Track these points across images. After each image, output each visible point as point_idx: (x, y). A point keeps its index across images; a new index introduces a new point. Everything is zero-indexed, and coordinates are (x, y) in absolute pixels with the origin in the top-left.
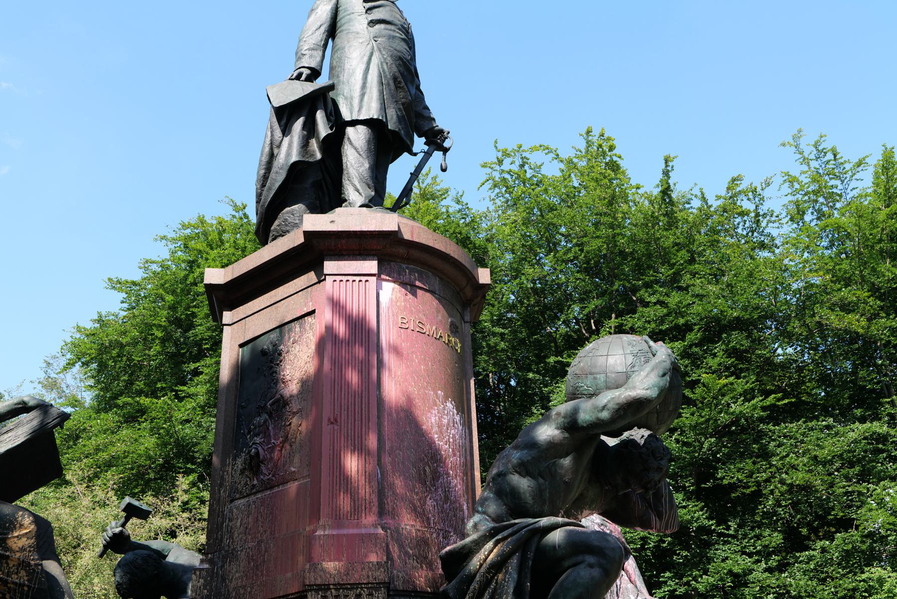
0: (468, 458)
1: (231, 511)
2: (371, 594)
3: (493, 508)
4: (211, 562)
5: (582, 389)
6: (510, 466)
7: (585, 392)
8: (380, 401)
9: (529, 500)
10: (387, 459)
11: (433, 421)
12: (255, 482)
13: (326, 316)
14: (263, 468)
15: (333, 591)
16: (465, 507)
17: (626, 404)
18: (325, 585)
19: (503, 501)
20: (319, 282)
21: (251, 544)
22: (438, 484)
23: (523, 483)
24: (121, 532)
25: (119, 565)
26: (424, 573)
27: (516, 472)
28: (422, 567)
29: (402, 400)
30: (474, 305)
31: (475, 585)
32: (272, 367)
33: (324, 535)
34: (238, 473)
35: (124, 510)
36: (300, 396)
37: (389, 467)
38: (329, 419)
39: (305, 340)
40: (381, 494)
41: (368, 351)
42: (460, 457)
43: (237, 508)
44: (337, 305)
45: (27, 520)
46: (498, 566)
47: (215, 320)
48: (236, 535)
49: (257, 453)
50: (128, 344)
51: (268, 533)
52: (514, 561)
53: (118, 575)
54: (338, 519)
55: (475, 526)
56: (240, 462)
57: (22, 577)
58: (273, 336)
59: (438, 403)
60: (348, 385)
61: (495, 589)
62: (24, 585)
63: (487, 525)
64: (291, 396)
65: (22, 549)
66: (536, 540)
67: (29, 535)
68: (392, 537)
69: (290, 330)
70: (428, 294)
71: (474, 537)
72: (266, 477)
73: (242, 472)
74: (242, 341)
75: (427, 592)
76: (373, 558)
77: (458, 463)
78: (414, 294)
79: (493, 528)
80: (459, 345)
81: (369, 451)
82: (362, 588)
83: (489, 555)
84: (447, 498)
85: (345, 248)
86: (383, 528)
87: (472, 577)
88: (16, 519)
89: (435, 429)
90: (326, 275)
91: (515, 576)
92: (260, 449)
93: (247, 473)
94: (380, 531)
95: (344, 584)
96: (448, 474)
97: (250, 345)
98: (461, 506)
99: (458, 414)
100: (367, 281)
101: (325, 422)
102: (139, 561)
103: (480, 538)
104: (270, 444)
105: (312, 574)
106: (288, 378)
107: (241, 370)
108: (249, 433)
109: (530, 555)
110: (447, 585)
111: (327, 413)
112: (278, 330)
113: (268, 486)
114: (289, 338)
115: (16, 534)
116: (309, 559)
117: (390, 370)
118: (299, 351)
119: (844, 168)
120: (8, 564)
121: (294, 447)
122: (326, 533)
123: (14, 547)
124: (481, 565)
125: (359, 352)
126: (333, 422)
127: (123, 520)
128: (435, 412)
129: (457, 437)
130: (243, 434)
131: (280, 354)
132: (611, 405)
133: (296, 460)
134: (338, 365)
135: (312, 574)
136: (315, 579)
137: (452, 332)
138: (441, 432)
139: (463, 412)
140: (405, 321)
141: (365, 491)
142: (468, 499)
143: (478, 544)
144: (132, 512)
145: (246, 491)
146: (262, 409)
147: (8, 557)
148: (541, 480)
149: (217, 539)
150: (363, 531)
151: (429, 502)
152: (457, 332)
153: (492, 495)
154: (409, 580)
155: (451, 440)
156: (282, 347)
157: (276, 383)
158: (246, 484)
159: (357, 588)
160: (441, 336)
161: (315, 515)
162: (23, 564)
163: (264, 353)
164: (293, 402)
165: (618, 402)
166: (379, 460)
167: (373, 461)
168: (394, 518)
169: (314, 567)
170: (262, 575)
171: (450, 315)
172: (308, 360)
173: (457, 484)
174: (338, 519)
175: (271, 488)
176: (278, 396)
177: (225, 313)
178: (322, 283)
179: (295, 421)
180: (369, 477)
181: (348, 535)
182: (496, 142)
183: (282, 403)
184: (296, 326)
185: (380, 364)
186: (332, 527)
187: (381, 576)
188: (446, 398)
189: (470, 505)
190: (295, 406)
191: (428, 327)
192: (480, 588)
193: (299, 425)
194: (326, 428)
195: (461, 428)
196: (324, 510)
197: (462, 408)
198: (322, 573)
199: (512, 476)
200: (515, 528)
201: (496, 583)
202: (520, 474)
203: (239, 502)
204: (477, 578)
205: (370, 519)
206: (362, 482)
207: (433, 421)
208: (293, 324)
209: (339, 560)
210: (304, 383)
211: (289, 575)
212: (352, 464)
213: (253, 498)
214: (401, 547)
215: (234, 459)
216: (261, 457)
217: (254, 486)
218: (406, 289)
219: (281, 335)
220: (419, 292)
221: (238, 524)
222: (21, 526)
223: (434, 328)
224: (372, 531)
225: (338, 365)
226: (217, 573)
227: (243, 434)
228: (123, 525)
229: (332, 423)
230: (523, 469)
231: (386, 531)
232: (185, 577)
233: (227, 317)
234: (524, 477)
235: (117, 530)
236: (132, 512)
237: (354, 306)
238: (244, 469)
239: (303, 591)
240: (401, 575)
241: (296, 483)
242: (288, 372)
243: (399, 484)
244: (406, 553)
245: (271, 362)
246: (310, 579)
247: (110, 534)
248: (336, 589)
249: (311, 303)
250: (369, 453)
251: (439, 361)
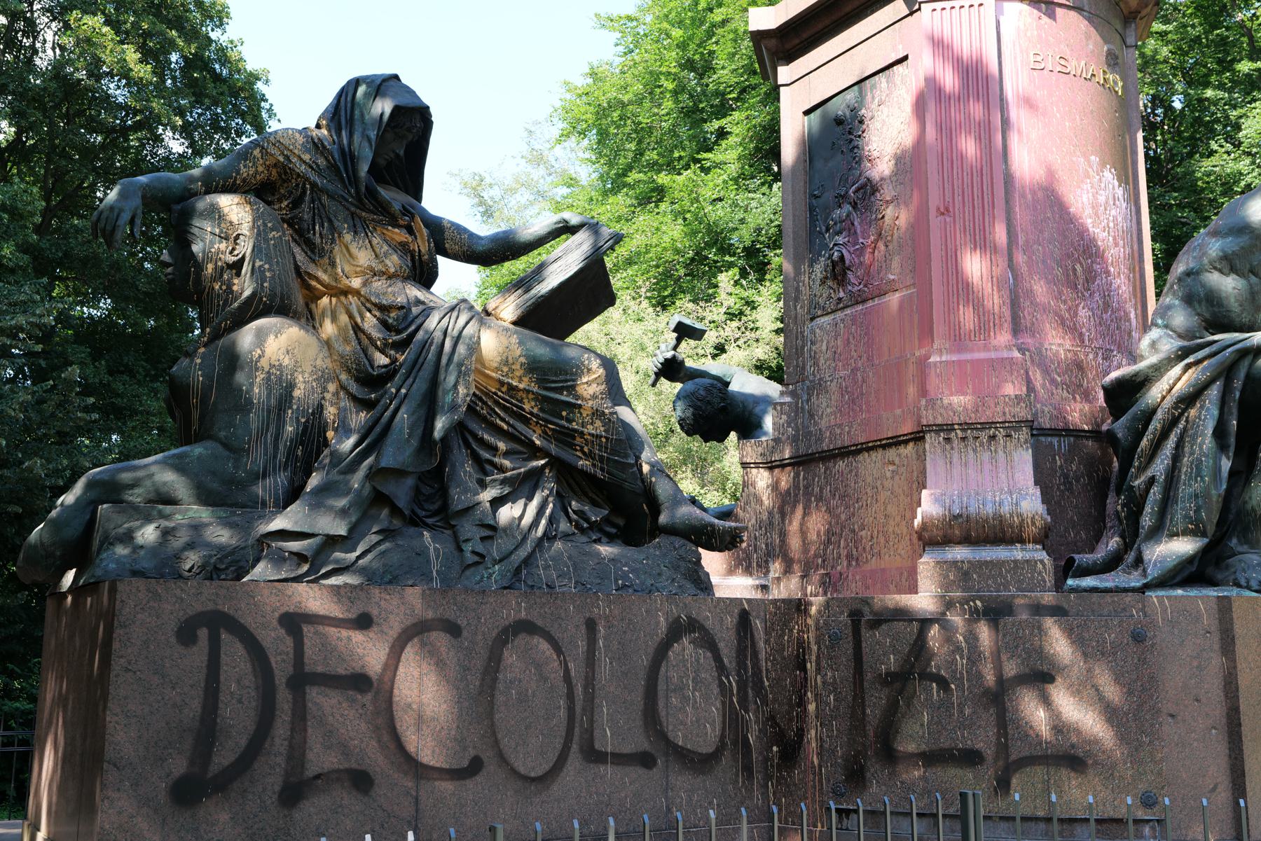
0: (1136, 247)
1: (813, 332)
2: (1009, 436)
3: (1181, 318)
4: (793, 394)
6: (1205, 261)
8: (1009, 179)
9: (1234, 306)
10: (1020, 258)
11: (1085, 200)
12: (842, 294)
13: (924, 63)
14: (850, 275)
15: (958, 432)
16: (1132, 315)
18: (947, 425)
19: (1195, 310)
20: (911, 14)
21: (842, 373)
22: (1094, 287)
23: (1228, 285)
24: (674, 356)
25: (678, 397)
26: (1078, 406)
27: (1215, 268)
28: (1074, 398)
29: (1040, 174)
30: (1141, 19)
31: (1155, 425)
32: (851, 140)
33: (941, 362)
34: (818, 282)
35: (674, 331)
36: (894, 179)
37: (1024, 269)
38: (938, 209)
40: (1015, 305)
41: (988, 107)
42: (1124, 247)
43: (821, 328)
44: (939, 45)
45: (595, 364)
46: (1190, 399)
47: (765, 77)
48: (822, 361)
49: (842, 258)
50: (630, 103)
51: (864, 358)
52: (1214, 392)
53: (678, 408)
54: (958, 340)
55: (1153, 344)
56: (819, 269)
57: (597, 428)
58: (850, 96)
59: (1091, 173)
60: (962, 157)
61: (1185, 430)
62: (601, 437)
63: (1169, 345)
64: (882, 179)
65: (594, 397)
66: (1246, 362)
67: (599, 381)
68: (1032, 361)
69: (873, 87)
70: (1073, 14)
71: (1153, 359)
72: (856, 288)
73: (823, 282)
75: (1084, 431)
76: (1010, 389)
77: (1122, 255)
78: (1052, 16)
79: (1181, 349)
80: (1120, 84)
81: (995, 245)
82: (996, 428)
83: (1175, 384)
84: (1107, 305)
86: (1019, 350)
87: (1150, 413)
88: (582, 363)
89: (1088, 211)
90: (920, 3)
91: (1216, 412)
92: (844, 251)
93: (830, 283)
94: (1016, 354)
95: (972, 424)
96: (1108, 273)
97: (818, 112)
98: (1127, 314)
99: (1120, 186)
101: (933, 212)
102: (702, 392)
103: (1160, 362)
104: (857, 243)
105: (930, 412)
106: (875, 154)
107: (811, 148)
108: (828, 230)
109: (1238, 384)
110: (1113, 423)
111: (934, 202)
112: (856, 88)
113: (860, 299)
114: (873, 98)
115: (585, 380)
116: (923, 392)
117: (1019, 131)
120: (581, 414)
121: (890, 247)
122: (944, 358)
123: (585, 394)
124: (1164, 398)
125: (976, 110)
126: (944, 211)
127: (674, 342)
128: (1087, 186)
129: (1120, 219)
130: (820, 232)
131: (861, 122)
133: (896, 263)
134: (947, 132)
135: (930, 412)
137: (1109, 65)
138: (1096, 215)
139: (1127, 183)
140: (1039, 59)
141: (995, 301)
142: (1135, 304)
143: (1159, 370)
144: (684, 332)
145: (830, 306)
146: (841, 199)
147: (580, 406)
148: (1253, 279)
149: (797, 366)
150: (993, 355)
151: (1083, 313)
152: (1117, 64)
153: (1177, 302)
154: (1060, 414)
155: (1111, 225)
156: (863, 111)
157: (859, 162)
158: (830, 297)
159: (990, 428)
160: (1093, 75)
161: (927, 332)
162: (598, 414)
163: (839, 121)
164: (885, 187)
166: (1010, 259)
167: (1002, 262)
168: (1034, 336)
169: (932, 403)
170: (861, 410)
171: (1106, 42)
172: (902, 127)
173: (1122, 284)
174: (958, 340)
175: (864, 301)
176: (862, 180)
177: (780, 69)
179: (889, 212)
180: (999, 284)
181: (972, 362)
183: (870, 189)
184: (881, 79)
185: (1006, 123)
186: (950, 351)
187: (1022, 412)
188: (1103, 165)
189: (1139, 312)
190: (887, 192)
191: (1074, 63)
192: (1163, 427)
193: (897, 217)
194: (935, 221)
195: (1124, 205)
196: (939, 328)
197: (1126, 177)
198: (942, 411)
199: (1208, 274)
200: (1214, 348)
201: (1187, 421)
202: (1220, 271)
203: (823, 319)
204: (1160, 414)
205: (1003, 337)
206: (988, 288)
207: (1085, 200)
208: (876, 78)
209: (964, 394)
210: (899, 159)
211: (898, 412)
212: (975, 266)
213: (839, 315)
214: (1046, 372)
215: (811, 266)
216: (847, 262)
217: (840, 299)
218: (1039, 10)
219: (861, 95)
220: (1060, 12)
221: (824, 348)
222: (589, 370)
223: (1083, 63)
224: (1005, 354)
225: (947, 132)
226: (803, 408)
227: (820, 232)
228: (675, 348)
229: (943, 214)
230: (1229, 264)
231: (1024, 354)
232: (757, 410)
233: (785, 73)
234: (1227, 275)
235: (669, 355)
236: (684, 332)
237: (965, 45)
238: (826, 278)
239: (918, 432)
240: (1046, 409)
241: (897, 295)
242: (875, 145)
243: (1040, 289)
244: (1053, 381)
245: (850, 133)
246: (928, 418)
247: (662, 360)
248: (963, 430)
250: (995, 250)
251: (1092, 112)
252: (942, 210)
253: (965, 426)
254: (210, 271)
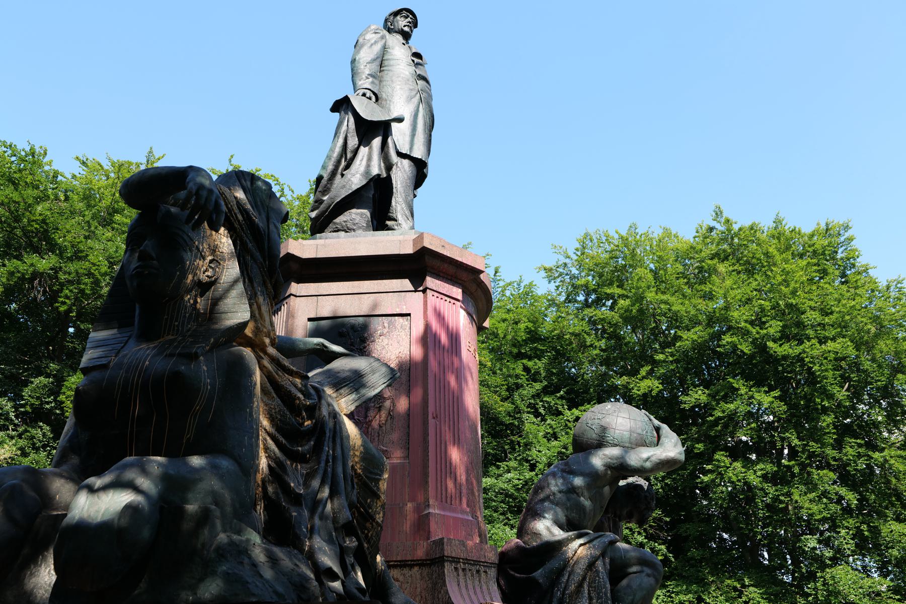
5: (608, 438)
7: (611, 442)
15: (461, 564)
18: (457, 558)
39: (395, 336)
74: (312, 316)
82: (480, 565)
95: (470, 560)
100: (454, 304)
118: (388, 344)
119: (499, 284)
120: (377, 504)
132: (654, 459)
136: (451, 552)
159: (477, 565)
165: (660, 458)
178: (417, 293)
181: (455, 518)
182: (232, 156)
198: (455, 548)
248: (464, 563)
249: (405, 307)
252: (435, 416)
253: (467, 561)
254: (189, 281)
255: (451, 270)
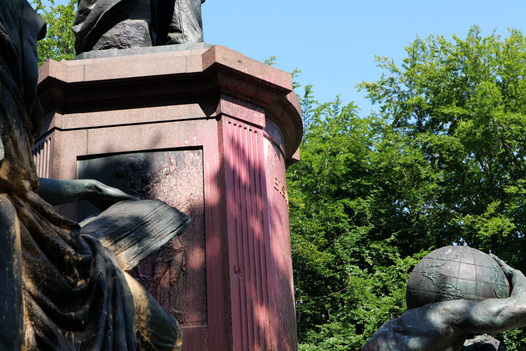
5: (449, 290)
7: (454, 294)
17: (520, 314)
39: (184, 175)
74: (82, 153)
85: (242, 92)
100: (255, 132)
118: (176, 185)
119: (311, 107)
132: (506, 312)
165: (513, 311)
178: (210, 120)
249: (195, 138)
252: (237, 270)
255: (251, 90)
